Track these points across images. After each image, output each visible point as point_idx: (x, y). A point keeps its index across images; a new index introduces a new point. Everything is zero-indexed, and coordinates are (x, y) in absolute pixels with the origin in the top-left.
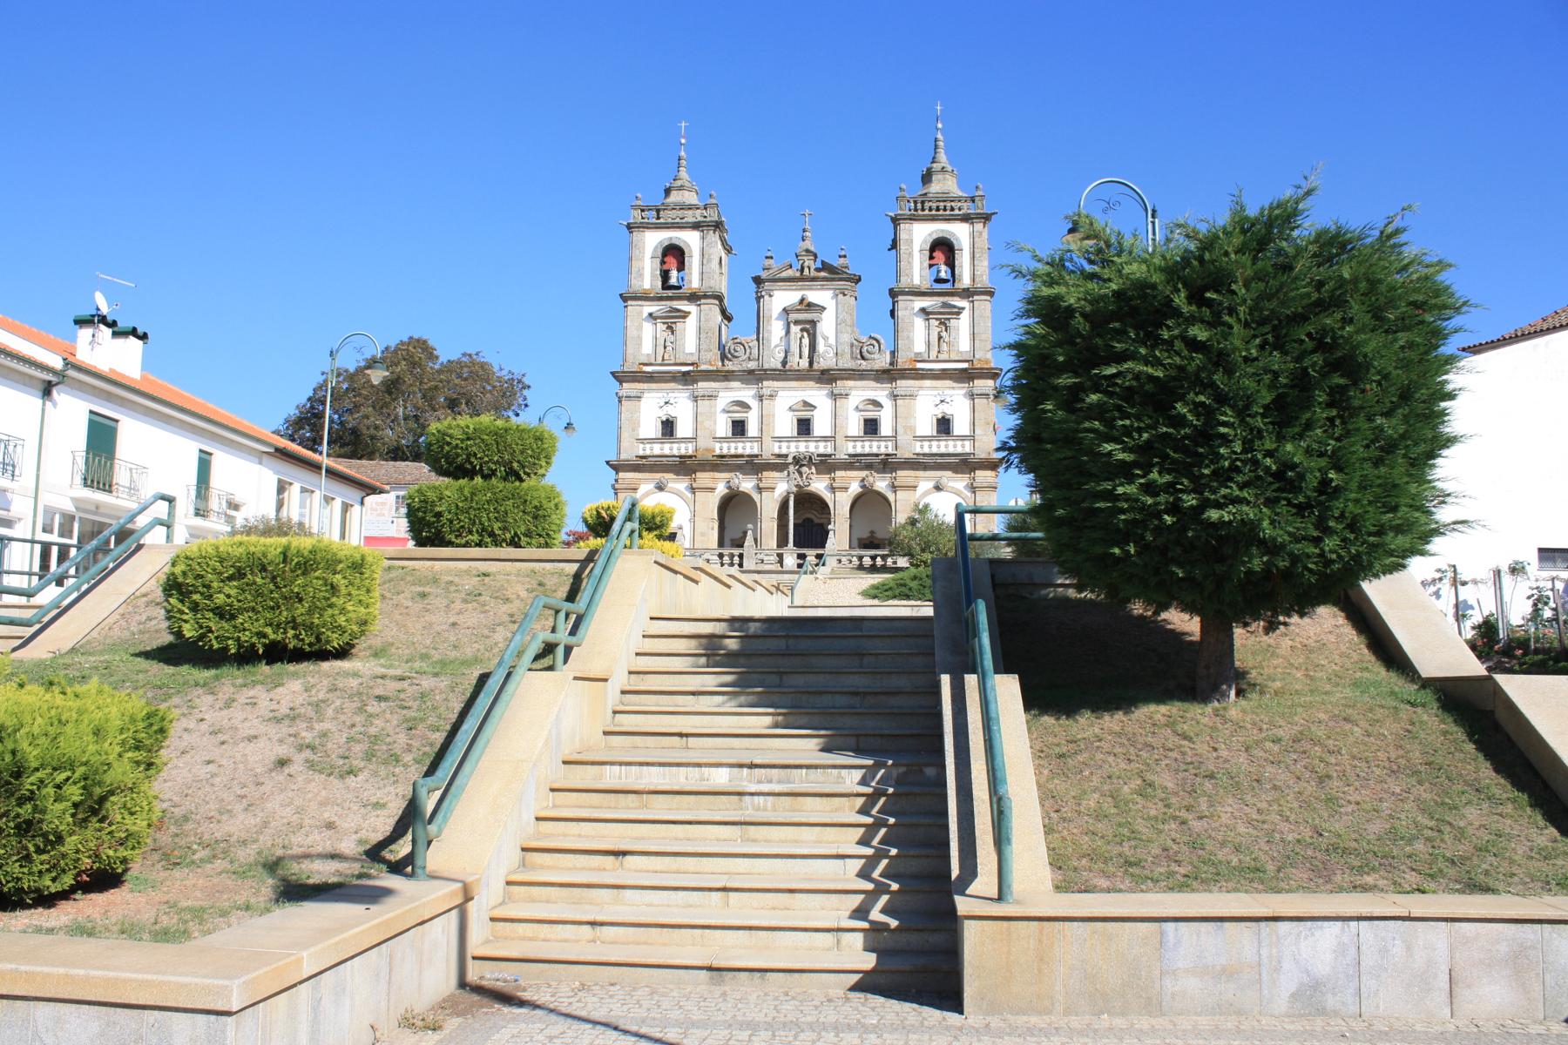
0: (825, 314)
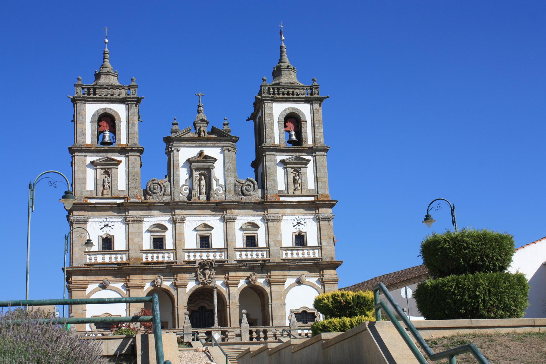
0: (216, 164)
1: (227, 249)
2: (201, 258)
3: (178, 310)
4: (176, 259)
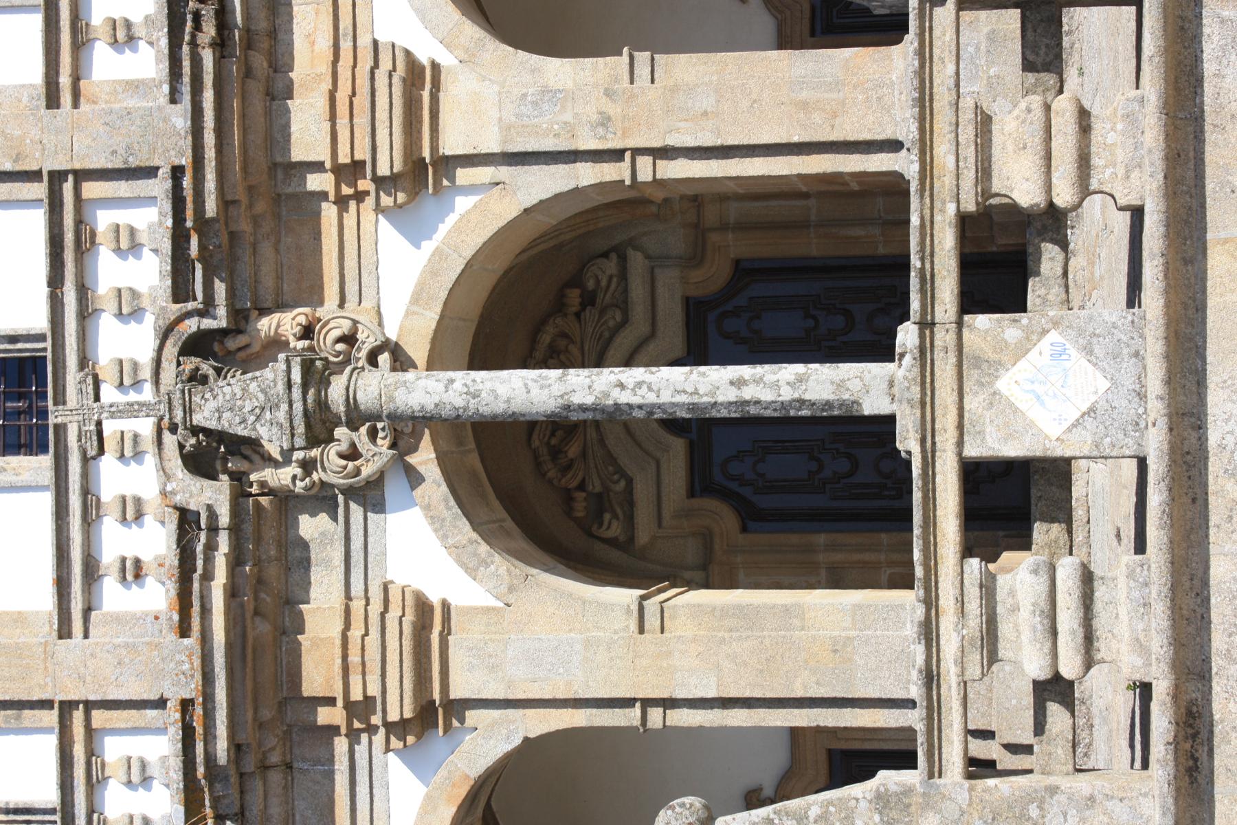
1: (57, 178)
2: (148, 444)
3: (669, 703)
4: (161, 703)
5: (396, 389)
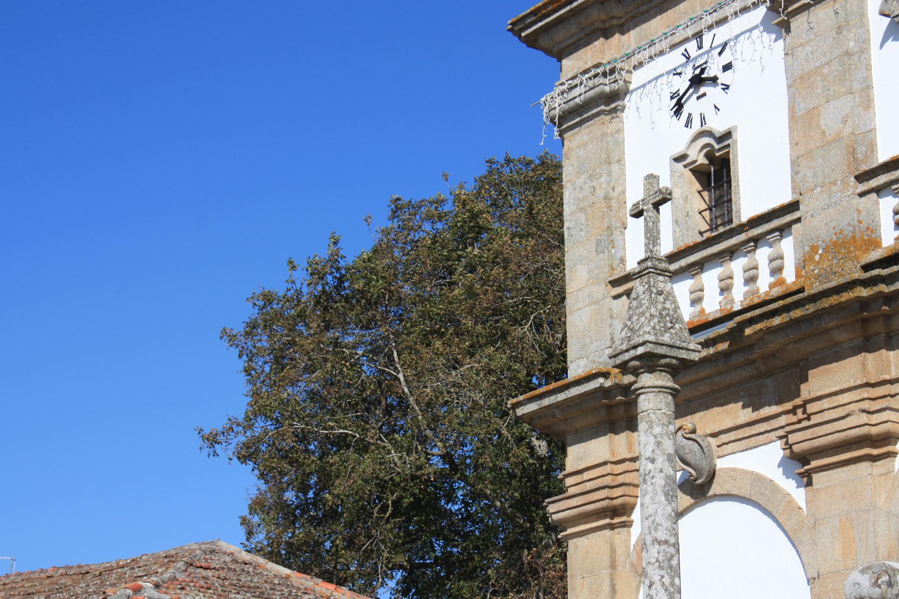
5: (647, 422)
